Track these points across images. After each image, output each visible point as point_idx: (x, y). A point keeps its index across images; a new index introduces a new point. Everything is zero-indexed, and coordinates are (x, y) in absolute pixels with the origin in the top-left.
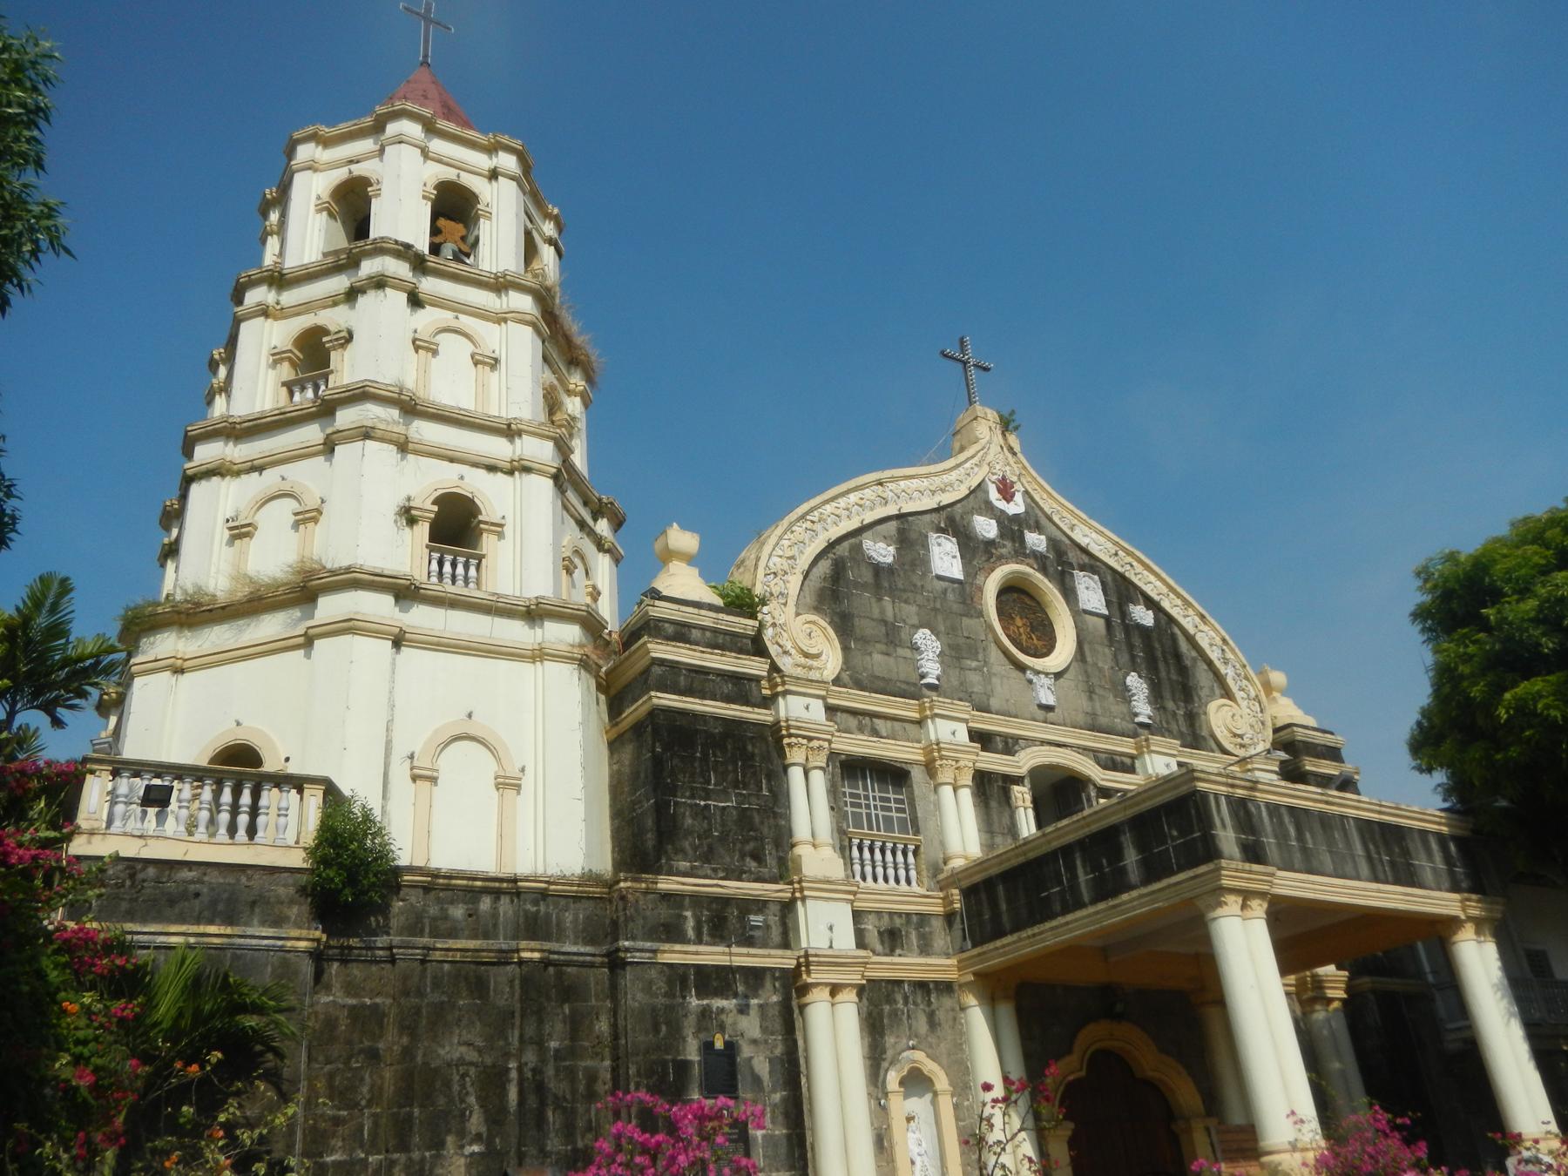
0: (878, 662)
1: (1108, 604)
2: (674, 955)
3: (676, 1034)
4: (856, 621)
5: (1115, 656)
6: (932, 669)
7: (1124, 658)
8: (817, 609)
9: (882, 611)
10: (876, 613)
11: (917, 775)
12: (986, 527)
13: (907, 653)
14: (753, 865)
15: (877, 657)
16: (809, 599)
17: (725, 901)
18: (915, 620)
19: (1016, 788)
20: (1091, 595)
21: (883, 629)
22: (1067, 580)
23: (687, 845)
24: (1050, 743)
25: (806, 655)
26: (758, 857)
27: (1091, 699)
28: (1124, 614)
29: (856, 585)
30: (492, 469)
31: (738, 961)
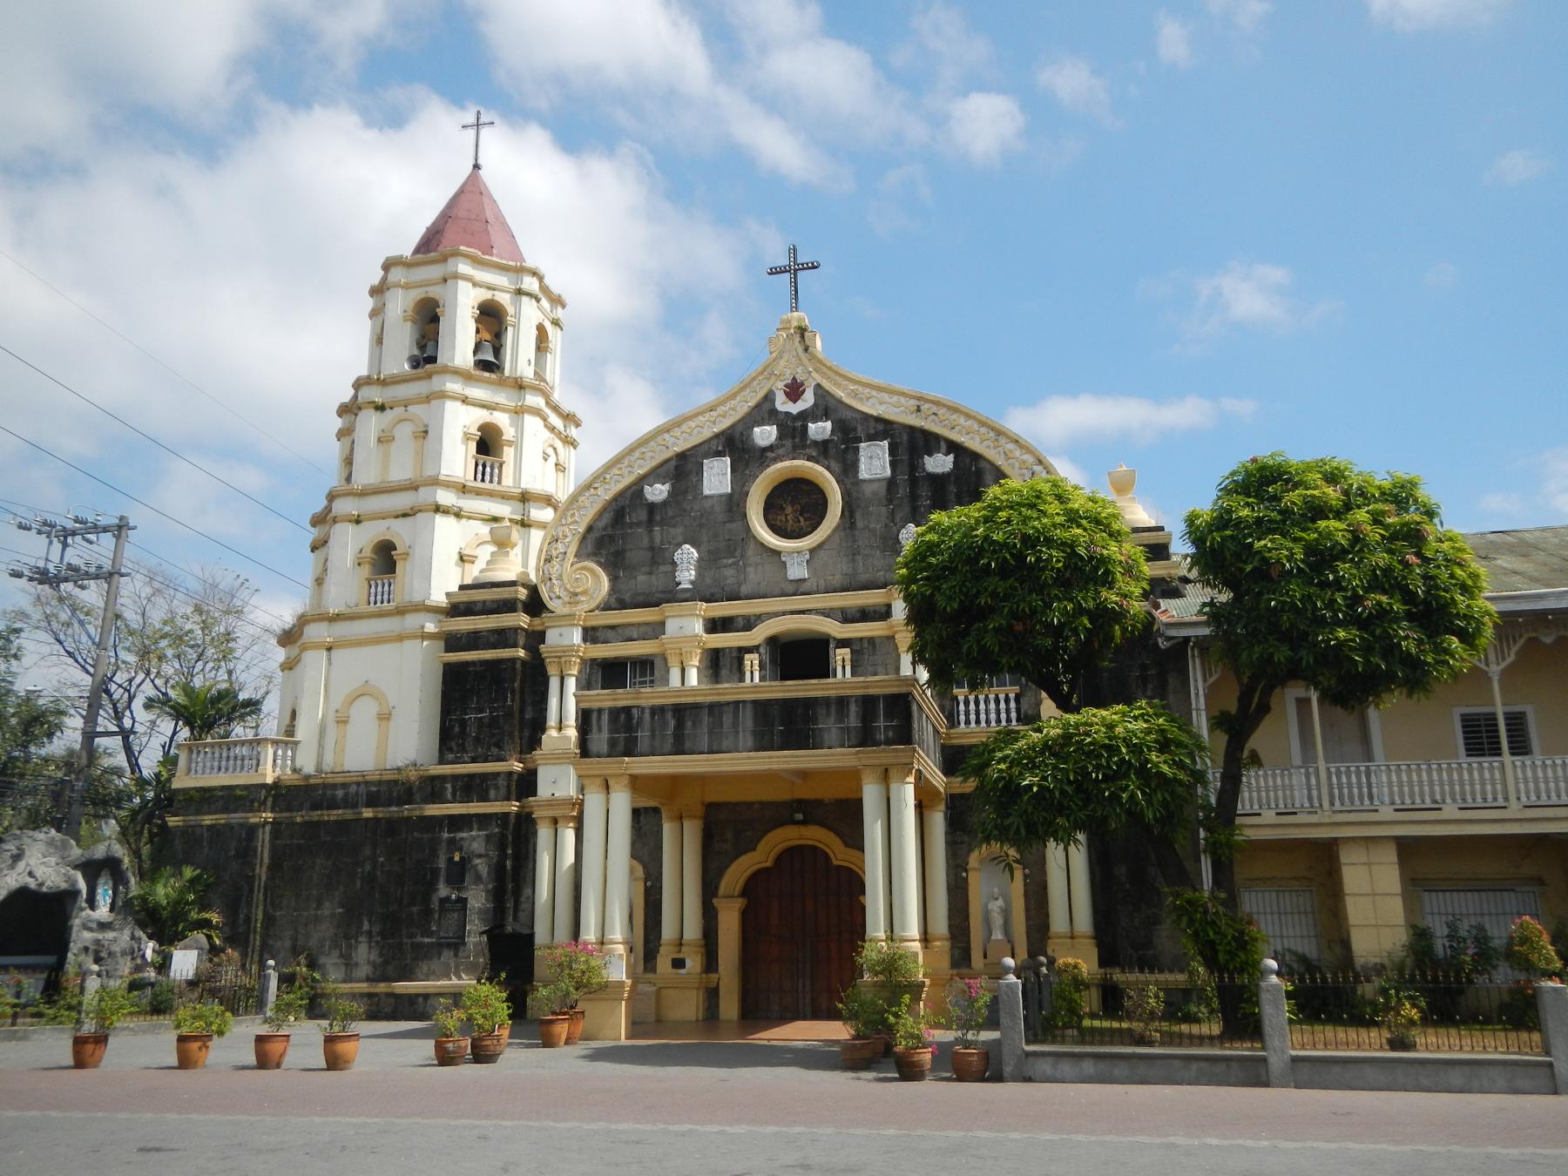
0: (642, 581)
1: (893, 464)
2: (433, 810)
3: (434, 854)
4: (628, 554)
5: (892, 514)
6: (687, 575)
7: (907, 509)
8: (594, 554)
9: (652, 540)
10: (646, 542)
11: (658, 663)
12: (765, 434)
13: (668, 568)
14: (495, 750)
15: (641, 578)
16: (590, 549)
17: (471, 776)
18: (680, 539)
19: (747, 656)
20: (875, 462)
21: (650, 554)
22: (850, 457)
23: (453, 744)
24: (793, 613)
25: (576, 595)
26: (499, 746)
27: (853, 560)
28: (914, 465)
29: (631, 525)
30: (405, 515)
31: (473, 811)
